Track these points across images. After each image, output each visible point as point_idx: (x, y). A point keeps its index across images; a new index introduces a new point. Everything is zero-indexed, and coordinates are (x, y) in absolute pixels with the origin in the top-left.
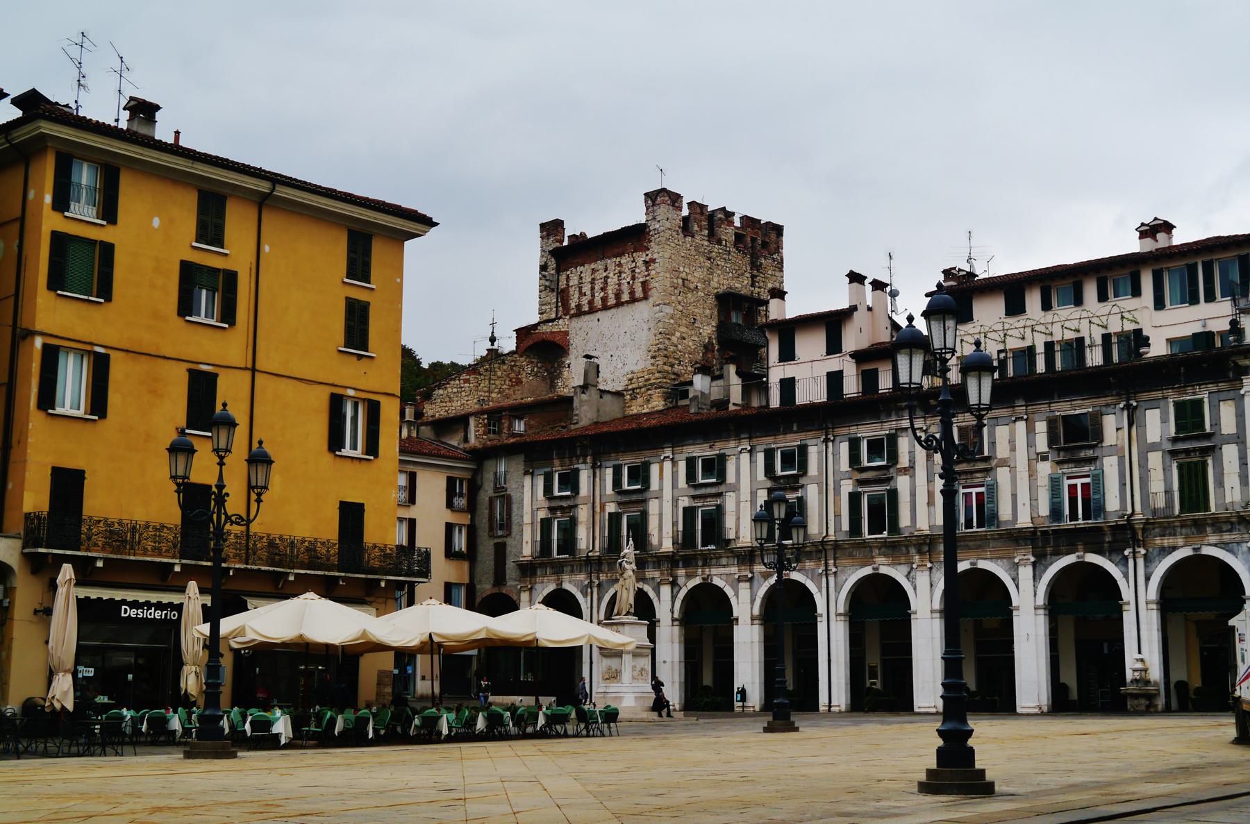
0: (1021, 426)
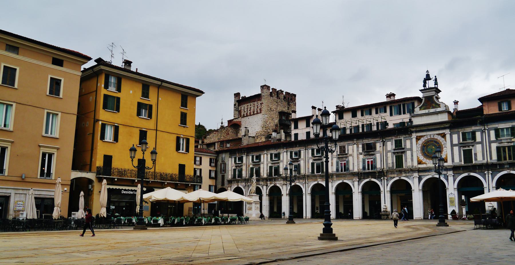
0: (355, 146)
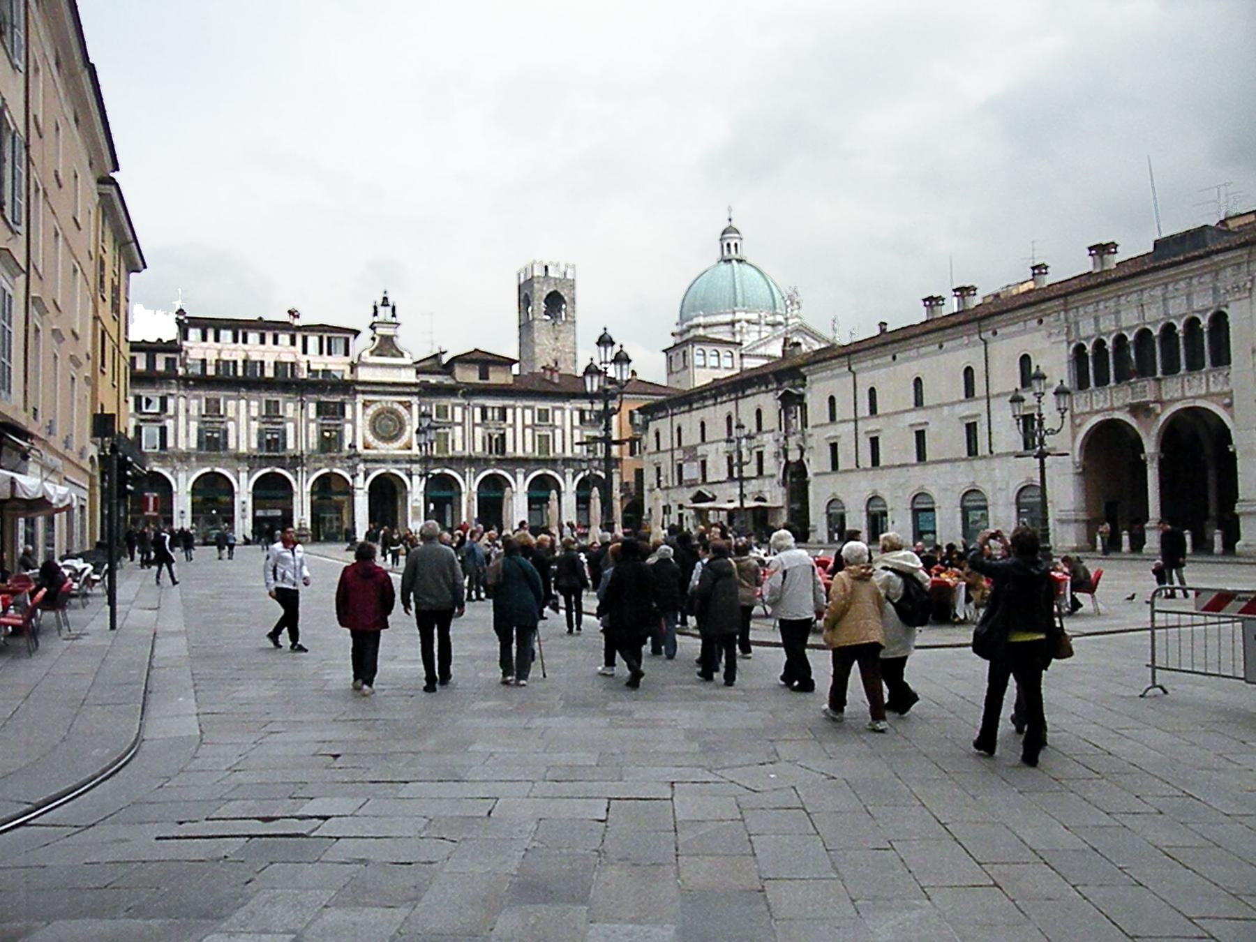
0: (243, 402)
